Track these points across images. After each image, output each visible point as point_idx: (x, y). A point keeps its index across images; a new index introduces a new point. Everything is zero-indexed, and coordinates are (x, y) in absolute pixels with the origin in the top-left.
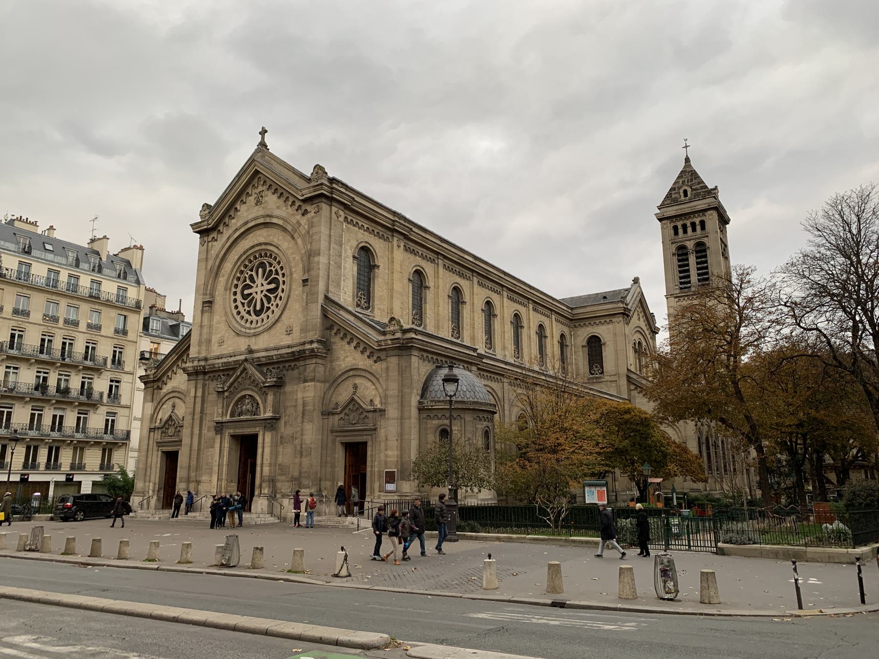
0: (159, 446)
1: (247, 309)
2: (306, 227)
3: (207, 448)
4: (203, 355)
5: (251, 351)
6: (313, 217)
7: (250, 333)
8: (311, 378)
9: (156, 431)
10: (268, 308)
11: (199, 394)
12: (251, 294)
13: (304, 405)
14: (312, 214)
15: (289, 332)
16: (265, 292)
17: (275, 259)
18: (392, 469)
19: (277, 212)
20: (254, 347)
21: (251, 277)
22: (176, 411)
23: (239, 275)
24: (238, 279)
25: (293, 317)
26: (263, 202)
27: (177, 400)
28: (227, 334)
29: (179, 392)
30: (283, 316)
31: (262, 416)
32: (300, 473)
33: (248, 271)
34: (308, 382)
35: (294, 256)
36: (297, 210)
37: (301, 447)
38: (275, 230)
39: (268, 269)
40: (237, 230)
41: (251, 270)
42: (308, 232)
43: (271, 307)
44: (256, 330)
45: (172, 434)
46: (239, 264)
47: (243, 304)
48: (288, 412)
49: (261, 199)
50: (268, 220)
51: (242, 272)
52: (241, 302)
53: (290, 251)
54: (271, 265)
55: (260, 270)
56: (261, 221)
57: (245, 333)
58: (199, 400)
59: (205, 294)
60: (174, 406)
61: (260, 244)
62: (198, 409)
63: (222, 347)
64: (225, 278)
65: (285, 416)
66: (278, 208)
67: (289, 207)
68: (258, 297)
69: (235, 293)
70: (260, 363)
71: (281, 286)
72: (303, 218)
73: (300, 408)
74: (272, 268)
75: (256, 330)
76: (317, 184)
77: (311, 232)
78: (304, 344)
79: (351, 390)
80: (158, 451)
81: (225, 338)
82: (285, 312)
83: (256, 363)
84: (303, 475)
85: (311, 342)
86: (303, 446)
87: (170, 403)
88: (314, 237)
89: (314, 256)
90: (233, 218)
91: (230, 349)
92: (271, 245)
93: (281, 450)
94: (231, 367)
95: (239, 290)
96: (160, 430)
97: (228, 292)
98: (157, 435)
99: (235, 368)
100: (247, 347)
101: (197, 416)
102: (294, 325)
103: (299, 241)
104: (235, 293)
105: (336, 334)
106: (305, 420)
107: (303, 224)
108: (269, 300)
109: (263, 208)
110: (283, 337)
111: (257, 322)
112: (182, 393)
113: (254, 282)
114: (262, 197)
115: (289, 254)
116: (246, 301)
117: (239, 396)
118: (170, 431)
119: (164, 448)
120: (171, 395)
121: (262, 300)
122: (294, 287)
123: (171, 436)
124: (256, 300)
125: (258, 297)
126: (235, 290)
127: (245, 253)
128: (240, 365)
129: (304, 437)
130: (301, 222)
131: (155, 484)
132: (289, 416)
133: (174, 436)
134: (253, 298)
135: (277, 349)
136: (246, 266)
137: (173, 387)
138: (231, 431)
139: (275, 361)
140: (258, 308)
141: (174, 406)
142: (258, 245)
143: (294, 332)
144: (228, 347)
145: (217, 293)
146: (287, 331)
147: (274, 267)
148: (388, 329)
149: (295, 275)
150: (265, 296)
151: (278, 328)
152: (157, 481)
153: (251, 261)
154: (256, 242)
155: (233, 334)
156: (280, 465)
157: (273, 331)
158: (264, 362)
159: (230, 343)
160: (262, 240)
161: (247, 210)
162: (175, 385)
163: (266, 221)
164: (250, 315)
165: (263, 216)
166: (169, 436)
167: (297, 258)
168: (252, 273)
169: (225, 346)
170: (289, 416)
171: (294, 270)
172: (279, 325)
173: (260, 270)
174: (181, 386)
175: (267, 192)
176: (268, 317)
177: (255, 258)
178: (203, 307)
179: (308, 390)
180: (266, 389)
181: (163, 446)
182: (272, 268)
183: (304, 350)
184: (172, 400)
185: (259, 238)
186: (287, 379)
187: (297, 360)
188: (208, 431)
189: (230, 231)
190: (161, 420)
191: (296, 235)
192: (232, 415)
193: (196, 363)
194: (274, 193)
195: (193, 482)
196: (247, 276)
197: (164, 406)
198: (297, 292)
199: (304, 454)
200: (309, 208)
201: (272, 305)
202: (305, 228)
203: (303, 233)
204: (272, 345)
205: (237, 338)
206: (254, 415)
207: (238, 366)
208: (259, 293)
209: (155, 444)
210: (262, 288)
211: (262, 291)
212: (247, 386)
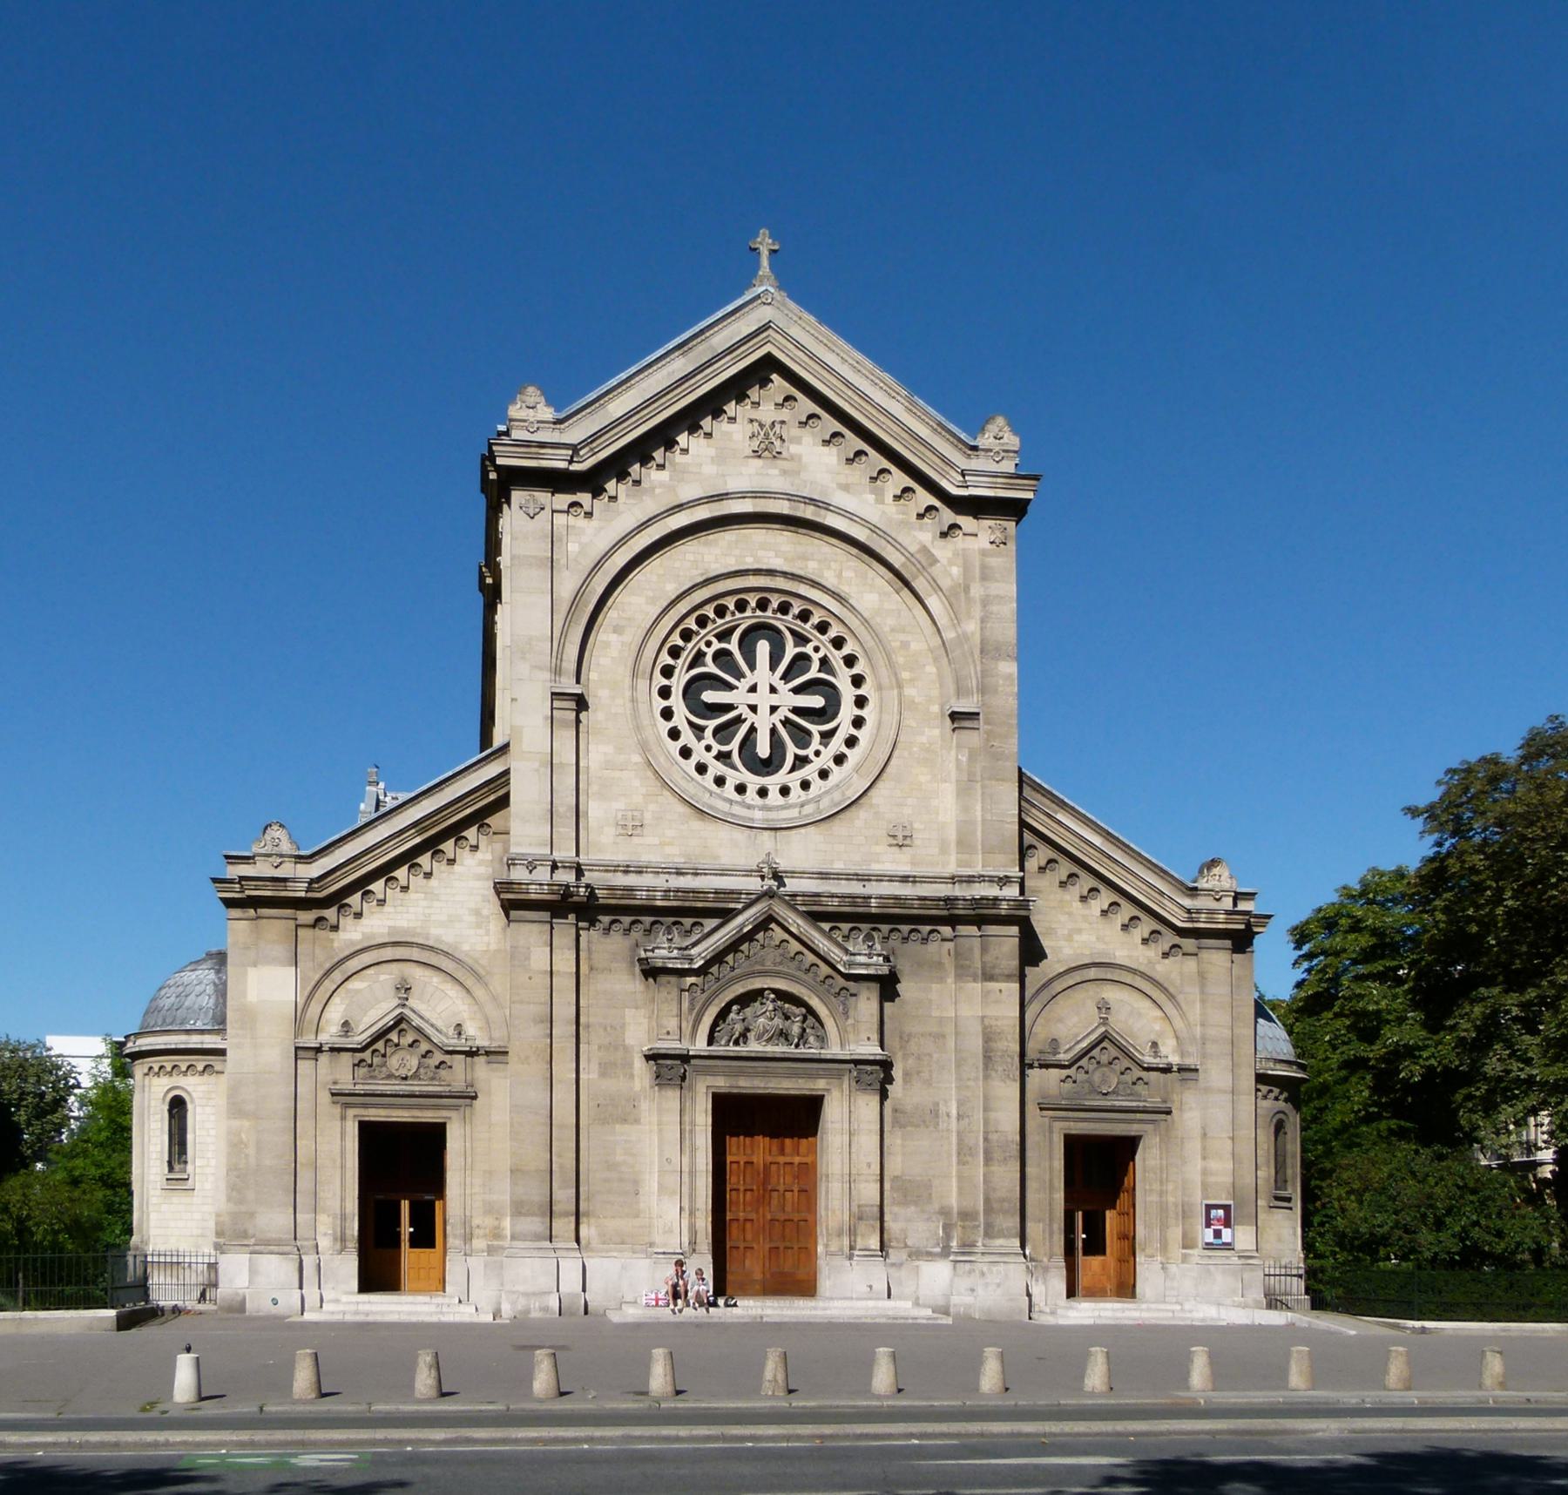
0: (347, 1106)
1: (716, 748)
2: (955, 570)
3: (604, 1122)
4: (565, 853)
5: (777, 876)
6: (984, 553)
7: (752, 820)
8: (1006, 972)
9: (324, 1058)
10: (801, 761)
11: (565, 962)
12: (729, 707)
13: (989, 1037)
14: (983, 541)
15: (901, 840)
16: (784, 712)
17: (823, 628)
18: (1221, 1199)
19: (839, 499)
20: (783, 864)
21: (722, 657)
22: (411, 1002)
23: (676, 640)
24: (675, 652)
25: (909, 801)
26: (785, 454)
27: (417, 974)
28: (652, 807)
29: (431, 948)
30: (872, 793)
31: (834, 1050)
32: (987, 1200)
33: (714, 640)
34: (997, 981)
35: (902, 637)
36: (920, 516)
37: (986, 1139)
38: (826, 549)
39: (791, 651)
40: (680, 507)
41: (724, 636)
42: (967, 589)
43: (812, 756)
44: (773, 815)
45: (403, 1072)
46: (683, 607)
47: (699, 730)
48: (913, 1047)
49: (777, 443)
50: (808, 513)
51: (687, 635)
52: (691, 723)
53: (890, 622)
54: (801, 639)
55: (763, 648)
56: (783, 507)
57: (733, 815)
58: (565, 985)
59: (557, 671)
60: (404, 989)
61: (771, 572)
62: (564, 1010)
63: (635, 840)
64: (633, 636)
65: (905, 1057)
66: (846, 488)
67: (889, 498)
68: (764, 723)
69: (665, 693)
70: (815, 908)
71: (847, 711)
72: (941, 542)
73: (976, 1044)
74: (809, 649)
75: (773, 815)
76: (993, 467)
77: (976, 591)
78: (970, 880)
79: (1094, 1016)
80: (343, 1118)
81: (648, 817)
82: (880, 784)
83: (804, 908)
84: (996, 1206)
85: (1004, 881)
86: (993, 1137)
87: (386, 977)
88: (994, 608)
89: (997, 658)
90: (661, 467)
91: (668, 850)
92: (815, 584)
93: (899, 1142)
94: (700, 905)
95: (678, 682)
96: (346, 1056)
97: (643, 684)
98: (342, 1072)
99: (735, 909)
100: (763, 857)
101: (564, 1030)
102: (916, 826)
103: (933, 602)
104: (665, 693)
105: (1042, 869)
106: (993, 1074)
107: (944, 561)
108: (802, 737)
109: (784, 472)
110: (878, 849)
111: (763, 792)
112: (446, 954)
113: (739, 675)
114: (784, 441)
115: (887, 629)
116: (712, 724)
117: (739, 989)
118: (394, 1062)
119: (372, 1111)
120: (388, 953)
121: (773, 731)
122: (910, 721)
123: (405, 1078)
124: (753, 729)
125: (764, 723)
126: (665, 682)
127: (708, 581)
128: (747, 906)
129: (992, 1115)
130: (937, 552)
131: (343, 1217)
132: (919, 1058)
133: (416, 1076)
134: (739, 720)
135: (864, 878)
136: (702, 622)
137: (392, 930)
138: (722, 1084)
139: (874, 910)
140: (763, 749)
141: (404, 989)
142: (757, 572)
143: (917, 842)
144: (662, 844)
145: (593, 676)
146: (894, 836)
147: (817, 649)
148: (1206, 886)
149: (909, 691)
150: (786, 722)
151: (858, 823)
152: (352, 1206)
153: (721, 611)
154: (750, 563)
155: (682, 809)
156: (896, 1177)
157: (838, 826)
158: (830, 909)
159: (670, 833)
160: (777, 563)
161: (720, 459)
162: (404, 924)
163: (799, 514)
164: (734, 768)
165: (790, 497)
166: (390, 1076)
167: (914, 646)
168: (724, 645)
169: (650, 839)
170: (919, 1058)
171: (905, 675)
172: (861, 815)
173: (763, 648)
174: (435, 931)
175: (792, 431)
176: (805, 785)
177: (741, 606)
178: (552, 709)
179: (997, 1002)
180: (851, 985)
181: (365, 1106)
182: (809, 649)
183: (996, 899)
184: (394, 966)
185: (761, 553)
186: (903, 966)
187: (953, 921)
188: (603, 1074)
189: (651, 507)
190: (346, 1024)
191: (920, 584)
192: (710, 1043)
193: (543, 874)
194: (826, 443)
195: (566, 1214)
196: (710, 652)
197: (354, 984)
198: (924, 739)
199: (997, 1155)
200: (966, 522)
201: (817, 753)
202: (950, 575)
203: (945, 583)
204: (838, 866)
205: (697, 824)
206: (797, 1046)
207: (740, 906)
208: (764, 709)
209: (325, 1097)
210: (774, 700)
211: (774, 709)
212: (769, 966)
